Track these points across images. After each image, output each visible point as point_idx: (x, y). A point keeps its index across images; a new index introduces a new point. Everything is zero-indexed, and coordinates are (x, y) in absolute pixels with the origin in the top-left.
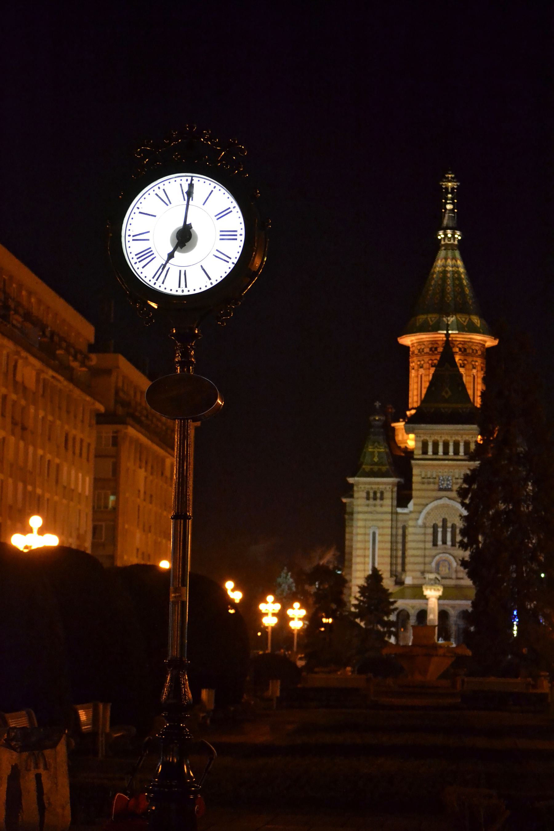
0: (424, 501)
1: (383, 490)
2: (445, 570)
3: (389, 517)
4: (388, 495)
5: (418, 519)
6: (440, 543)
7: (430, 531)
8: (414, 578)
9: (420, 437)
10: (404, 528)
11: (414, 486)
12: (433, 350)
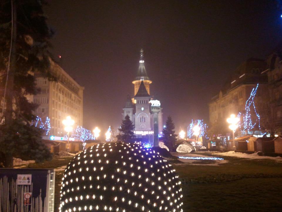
4: (131, 112)
7: (140, 119)
11: (136, 110)
12: (139, 84)
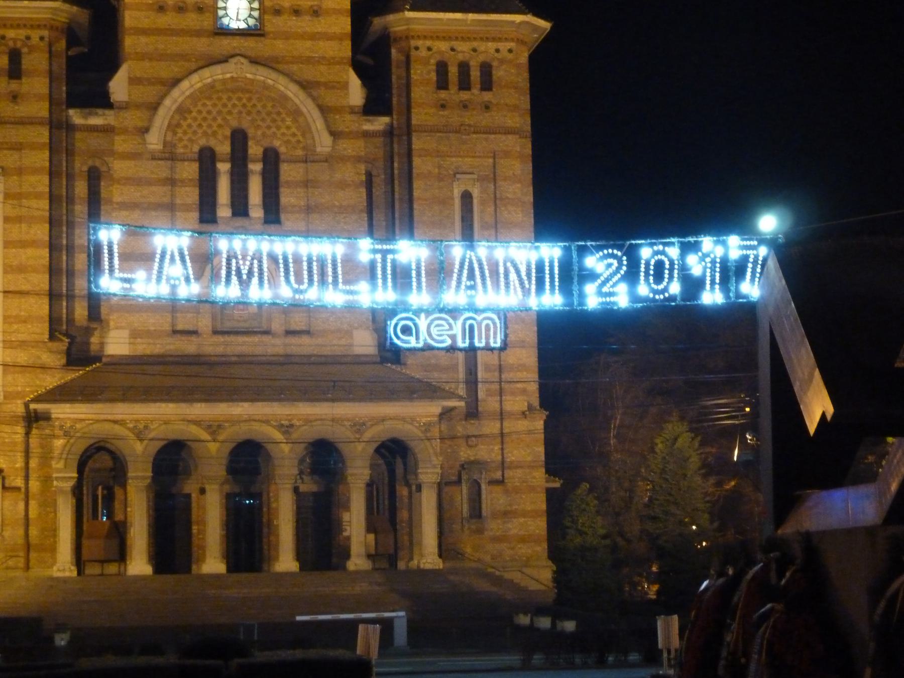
0: (166, 71)
1: (19, 44)
3: (42, 135)
5: (146, 130)
7: (190, 170)
8: (135, 334)
10: (94, 177)
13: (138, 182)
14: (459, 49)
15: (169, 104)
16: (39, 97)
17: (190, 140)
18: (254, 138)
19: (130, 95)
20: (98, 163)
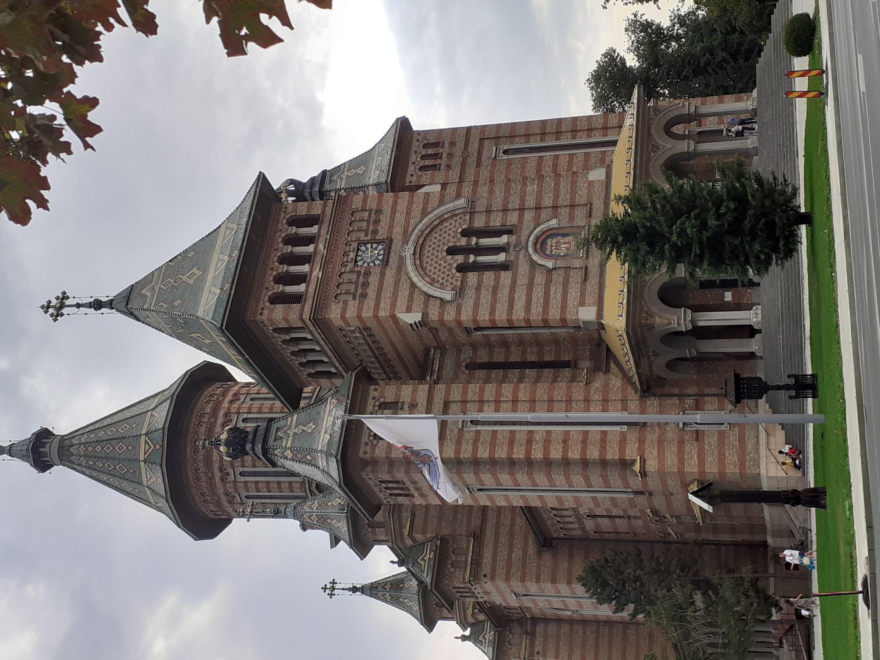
0: (404, 292)
1: (377, 404)
2: (569, 243)
6: (501, 257)
7: (472, 277)
8: (582, 303)
9: (263, 309)
13: (476, 305)
14: (414, 160)
15: (426, 288)
16: (415, 391)
17: (452, 278)
18: (455, 242)
19: (418, 312)
20: (464, 364)
